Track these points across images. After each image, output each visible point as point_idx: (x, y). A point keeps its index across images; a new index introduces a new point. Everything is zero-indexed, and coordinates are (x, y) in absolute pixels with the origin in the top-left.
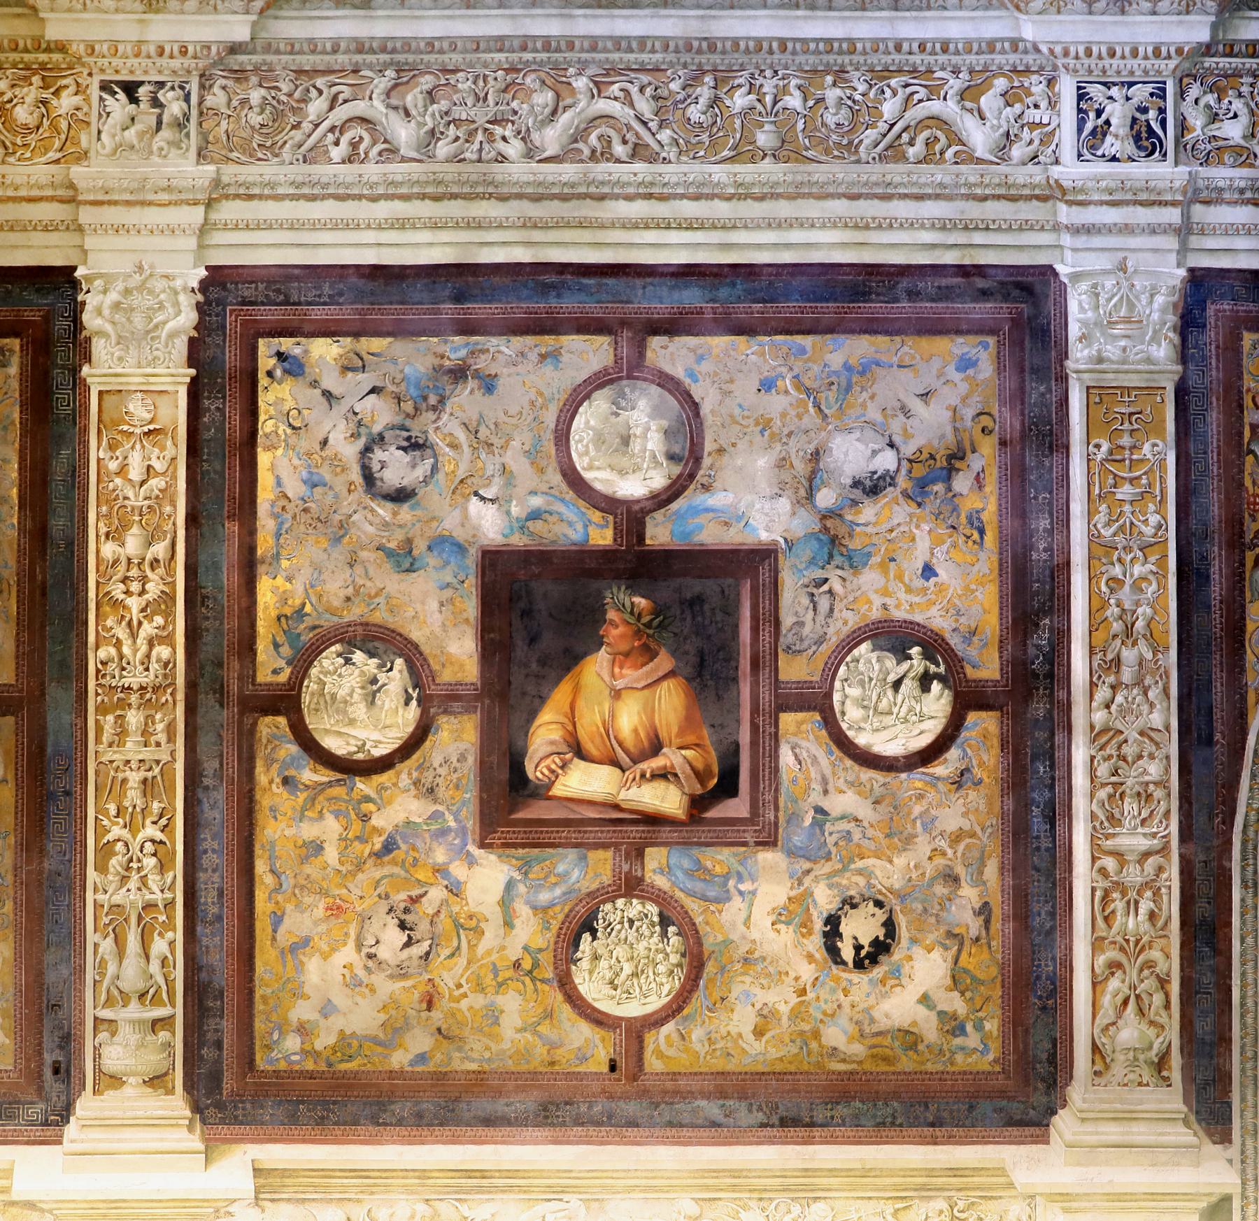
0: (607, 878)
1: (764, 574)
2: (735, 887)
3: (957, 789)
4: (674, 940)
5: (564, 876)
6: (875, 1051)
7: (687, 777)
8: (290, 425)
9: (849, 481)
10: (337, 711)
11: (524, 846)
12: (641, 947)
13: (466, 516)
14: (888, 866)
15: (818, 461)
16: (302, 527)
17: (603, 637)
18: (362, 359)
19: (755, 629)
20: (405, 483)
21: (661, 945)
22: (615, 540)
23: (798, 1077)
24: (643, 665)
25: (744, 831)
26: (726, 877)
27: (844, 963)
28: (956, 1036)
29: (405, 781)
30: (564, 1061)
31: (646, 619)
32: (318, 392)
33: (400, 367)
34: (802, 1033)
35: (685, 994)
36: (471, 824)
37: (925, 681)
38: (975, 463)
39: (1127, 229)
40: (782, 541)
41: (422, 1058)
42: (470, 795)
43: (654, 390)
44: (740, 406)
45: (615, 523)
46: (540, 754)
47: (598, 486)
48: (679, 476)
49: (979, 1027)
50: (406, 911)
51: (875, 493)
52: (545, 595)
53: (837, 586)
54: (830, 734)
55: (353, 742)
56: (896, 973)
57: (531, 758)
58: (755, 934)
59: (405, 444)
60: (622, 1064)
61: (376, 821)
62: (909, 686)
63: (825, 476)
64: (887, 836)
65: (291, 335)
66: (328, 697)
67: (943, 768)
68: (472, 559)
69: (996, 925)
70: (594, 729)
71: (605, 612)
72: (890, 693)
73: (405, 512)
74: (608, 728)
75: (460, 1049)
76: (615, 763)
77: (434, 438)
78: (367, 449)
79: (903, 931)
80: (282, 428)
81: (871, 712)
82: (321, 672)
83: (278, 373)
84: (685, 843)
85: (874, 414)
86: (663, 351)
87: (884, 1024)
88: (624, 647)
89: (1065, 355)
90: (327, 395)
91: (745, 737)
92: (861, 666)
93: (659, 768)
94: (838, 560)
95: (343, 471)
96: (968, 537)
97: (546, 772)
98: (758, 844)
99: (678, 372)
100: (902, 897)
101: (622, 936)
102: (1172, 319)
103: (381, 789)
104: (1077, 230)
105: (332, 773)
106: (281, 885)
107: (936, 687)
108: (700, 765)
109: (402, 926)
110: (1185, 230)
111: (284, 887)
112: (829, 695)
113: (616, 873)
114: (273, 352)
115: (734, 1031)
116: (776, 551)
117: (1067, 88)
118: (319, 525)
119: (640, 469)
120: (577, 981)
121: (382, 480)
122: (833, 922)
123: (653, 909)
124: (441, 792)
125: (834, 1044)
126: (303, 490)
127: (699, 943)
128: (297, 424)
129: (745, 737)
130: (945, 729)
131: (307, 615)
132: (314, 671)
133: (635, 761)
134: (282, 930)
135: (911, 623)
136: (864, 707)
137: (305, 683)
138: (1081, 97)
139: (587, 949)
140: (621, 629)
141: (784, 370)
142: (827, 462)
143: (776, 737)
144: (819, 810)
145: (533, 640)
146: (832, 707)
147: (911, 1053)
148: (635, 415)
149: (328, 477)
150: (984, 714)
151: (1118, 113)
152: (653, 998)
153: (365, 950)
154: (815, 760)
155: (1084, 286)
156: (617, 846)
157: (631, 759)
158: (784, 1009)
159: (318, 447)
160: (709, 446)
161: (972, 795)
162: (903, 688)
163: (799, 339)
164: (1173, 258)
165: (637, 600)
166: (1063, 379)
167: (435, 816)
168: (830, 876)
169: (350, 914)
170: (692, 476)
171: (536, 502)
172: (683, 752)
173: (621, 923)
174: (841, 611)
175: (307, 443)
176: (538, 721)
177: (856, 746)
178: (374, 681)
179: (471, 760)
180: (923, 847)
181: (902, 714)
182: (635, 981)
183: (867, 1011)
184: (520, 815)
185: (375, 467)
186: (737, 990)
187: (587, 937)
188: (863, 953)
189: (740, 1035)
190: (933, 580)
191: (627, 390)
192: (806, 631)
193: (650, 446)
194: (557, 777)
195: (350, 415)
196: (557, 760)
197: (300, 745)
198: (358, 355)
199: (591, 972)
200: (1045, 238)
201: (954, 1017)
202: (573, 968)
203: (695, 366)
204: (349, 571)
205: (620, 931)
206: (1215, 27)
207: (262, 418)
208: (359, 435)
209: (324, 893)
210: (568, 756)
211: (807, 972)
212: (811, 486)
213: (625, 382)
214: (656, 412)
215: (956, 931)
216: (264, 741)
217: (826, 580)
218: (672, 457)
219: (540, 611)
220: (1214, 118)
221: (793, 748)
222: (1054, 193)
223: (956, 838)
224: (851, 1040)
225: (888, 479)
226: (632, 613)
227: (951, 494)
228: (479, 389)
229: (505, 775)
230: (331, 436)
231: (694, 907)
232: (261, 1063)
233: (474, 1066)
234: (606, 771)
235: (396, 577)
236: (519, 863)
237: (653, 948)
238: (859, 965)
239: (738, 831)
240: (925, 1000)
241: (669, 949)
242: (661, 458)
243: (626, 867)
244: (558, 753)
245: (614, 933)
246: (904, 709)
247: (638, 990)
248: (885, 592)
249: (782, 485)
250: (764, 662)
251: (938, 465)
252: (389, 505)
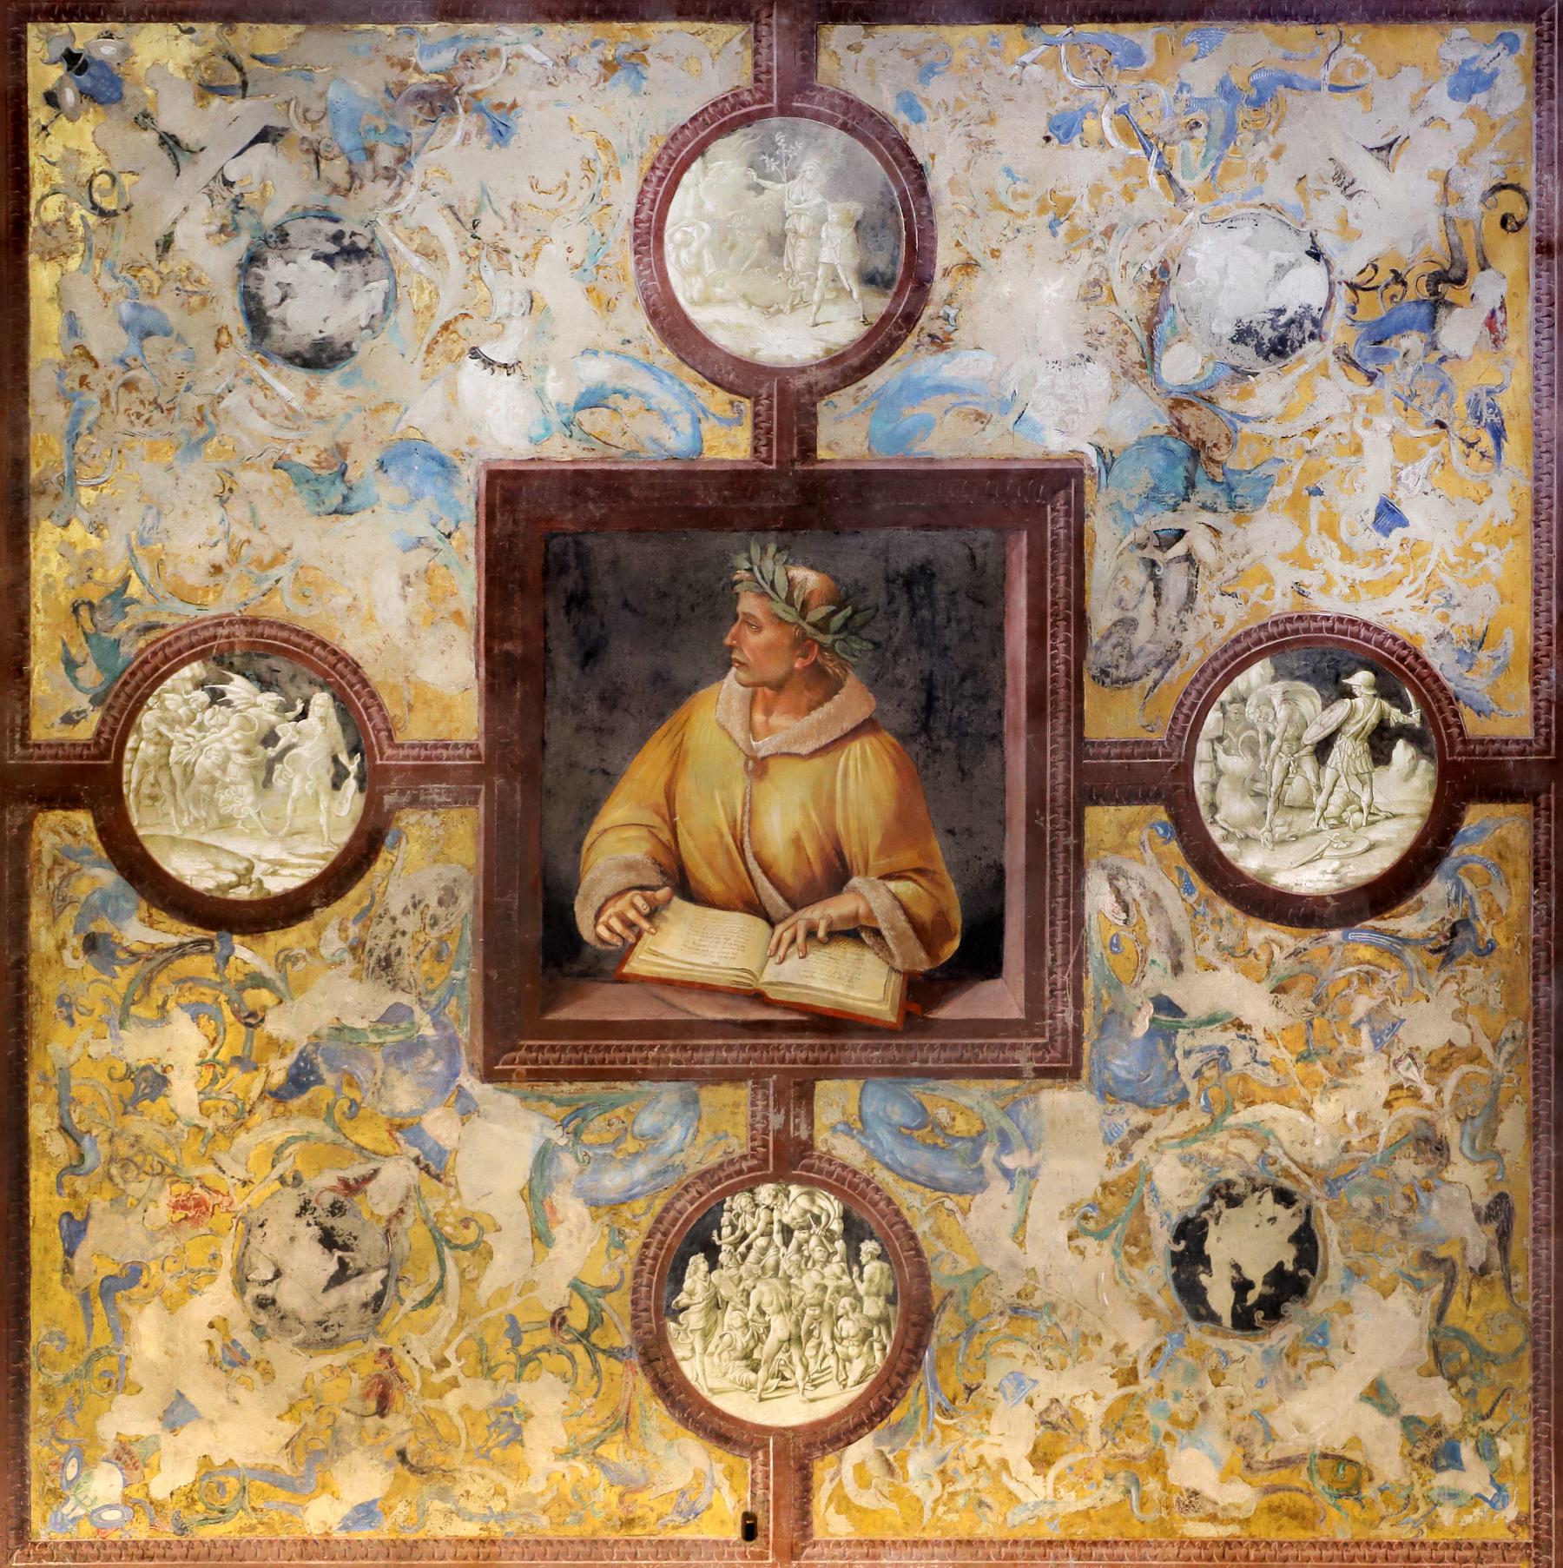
0: (738, 1143)
1: (1056, 525)
2: (996, 1162)
3: (1444, 963)
4: (873, 1268)
5: (652, 1140)
6: (1275, 1498)
7: (899, 938)
8: (95, 207)
9: (1229, 330)
10: (196, 800)
11: (571, 1076)
12: (807, 1283)
13: (453, 397)
14: (1303, 1118)
15: (1164, 286)
16: (122, 422)
17: (731, 649)
18: (240, 69)
19: (1037, 635)
20: (330, 330)
21: (846, 1279)
22: (756, 450)
23: (1119, 1550)
24: (811, 708)
25: (1014, 1047)
26: (978, 1141)
27: (1213, 1318)
28: (1438, 1469)
29: (332, 943)
30: (652, 1517)
31: (816, 614)
32: (151, 137)
33: (319, 87)
34: (1130, 1459)
35: (895, 1380)
36: (467, 1032)
37: (1380, 741)
38: (1487, 289)
40: (1091, 453)
41: (367, 1512)
42: (465, 972)
43: (835, 137)
44: (1008, 172)
45: (756, 415)
46: (606, 889)
47: (721, 338)
48: (885, 319)
49: (1486, 1451)
50: (336, 1209)
51: (1281, 354)
52: (615, 563)
53: (1200, 542)
54: (1188, 851)
55: (227, 863)
56: (1318, 1338)
57: (586, 897)
58: (1034, 1258)
59: (332, 248)
60: (767, 1522)
61: (275, 1025)
62: (1347, 751)
63: (1181, 318)
64: (1302, 1058)
65: (95, 17)
66: (176, 772)
67: (1408, 922)
68: (467, 491)
69: (1522, 1241)
70: (715, 838)
71: (735, 599)
72: (1308, 765)
73: (331, 383)
74: (741, 836)
75: (443, 1495)
76: (754, 907)
77: (387, 235)
78: (254, 259)
79: (1334, 1254)
80: (79, 213)
81: (1270, 806)
82: (162, 720)
83: (69, 96)
84: (895, 1072)
85: (1280, 188)
86: (853, 56)
87: (1292, 1443)
88: (776, 670)
90: (170, 143)
91: (1015, 856)
92: (1251, 712)
93: (842, 919)
94: (1205, 491)
95: (204, 303)
96: (1471, 445)
97: (617, 925)
98: (1041, 1073)
99: (883, 100)
100: (1332, 1182)
101: (770, 1260)
103: (285, 959)
105: (185, 927)
106: (82, 1157)
107: (1402, 752)
108: (925, 913)
109: (328, 1240)
111: (89, 1161)
112: (1185, 770)
113: (758, 1133)
114: (59, 51)
115: (991, 1455)
116: (1079, 474)
118: (157, 415)
119: (805, 303)
120: (678, 1353)
121: (284, 323)
122: (1191, 1232)
123: (830, 1206)
124: (407, 967)
125: (1192, 1483)
126: (122, 342)
127: (923, 1276)
128: (108, 204)
129: (1015, 856)
130: (1420, 840)
131: (133, 601)
132: (147, 718)
133: (795, 905)
134: (84, 1250)
135: (1353, 622)
136: (1257, 795)
137: (131, 743)
139: (699, 1288)
140: (769, 634)
141: (1098, 96)
142: (1182, 288)
143: (1077, 857)
144: (1164, 1005)
145: (590, 654)
146: (1190, 795)
147: (1348, 1503)
148: (796, 189)
149: (173, 317)
150: (1498, 810)
152: (831, 1388)
153: (253, 1291)
154: (1156, 901)
156: (758, 1077)
157: (788, 900)
158: (1092, 1411)
159: (152, 255)
160: (945, 256)
161: (1475, 974)
162: (1335, 756)
163: (1129, 32)
165: (800, 573)
167: (394, 1016)
168: (1184, 1139)
169: (222, 1219)
170: (910, 319)
171: (597, 371)
172: (892, 885)
173: (767, 1233)
174: (1211, 597)
175: (132, 244)
176: (602, 822)
177: (1239, 875)
178: (270, 738)
179: (466, 901)
180: (1373, 1080)
181: (1332, 810)
182: (795, 1352)
183: (1259, 1415)
184: (566, 1014)
185: (270, 295)
186: (997, 1372)
187: (698, 1262)
188: (1252, 1297)
189: (1004, 1464)
190: (1398, 533)
191: (780, 138)
192: (1141, 637)
193: (826, 256)
194: (639, 936)
195: (218, 186)
196: (639, 901)
197: (121, 870)
198: (231, 60)
199: (706, 1335)
201: (1436, 1430)
202: (672, 1325)
203: (917, 89)
204: (218, 513)
205: (764, 1251)
207: (37, 191)
208: (237, 228)
209: (168, 1173)
210: (662, 893)
211: (1138, 1336)
212: (1151, 340)
213: (775, 121)
214: (841, 182)
215: (1441, 1253)
216: (47, 861)
217: (1181, 534)
218: (870, 279)
219: (604, 596)
221: (1112, 879)
223: (1441, 1063)
224: (1227, 1475)
225: (1308, 326)
226: (789, 601)
227: (1437, 355)
228: (480, 132)
229: (532, 932)
230: (179, 232)
231: (912, 1201)
232: (42, 1528)
233: (471, 1530)
234: (738, 922)
235: (314, 524)
236: (563, 1112)
237: (831, 1284)
238: (1244, 1321)
239: (1002, 1047)
240: (1377, 1394)
241: (862, 1288)
242: (850, 282)
243: (776, 1121)
244: (642, 888)
245: (753, 1255)
246: (1337, 799)
247: (799, 1370)
248: (1300, 559)
249: (1093, 337)
250: (1055, 703)
251: (1411, 295)
252: (300, 375)
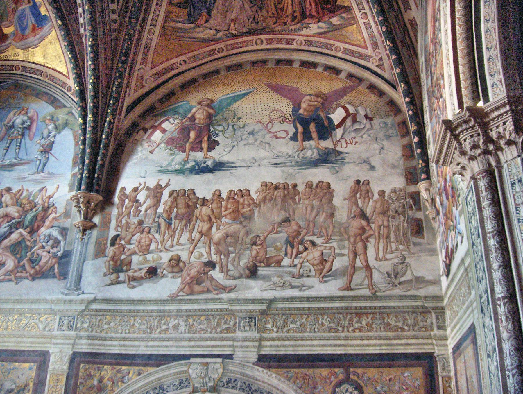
39: (63, 344)
89: (48, 367)
102: (69, 361)
104: (54, 344)
110: (74, 344)
117: (58, 317)
138: (60, 319)
151: (66, 322)
155: (54, 355)
164: (70, 350)
166: (47, 372)
200: (49, 345)
206: (86, 306)
220: (83, 323)
222: (51, 337)
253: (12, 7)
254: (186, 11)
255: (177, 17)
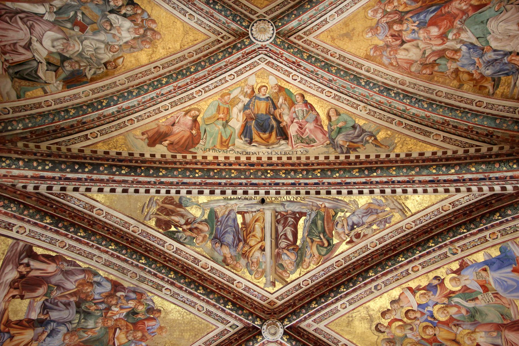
253: (492, 296)
254: (503, 78)
255: (509, 87)
